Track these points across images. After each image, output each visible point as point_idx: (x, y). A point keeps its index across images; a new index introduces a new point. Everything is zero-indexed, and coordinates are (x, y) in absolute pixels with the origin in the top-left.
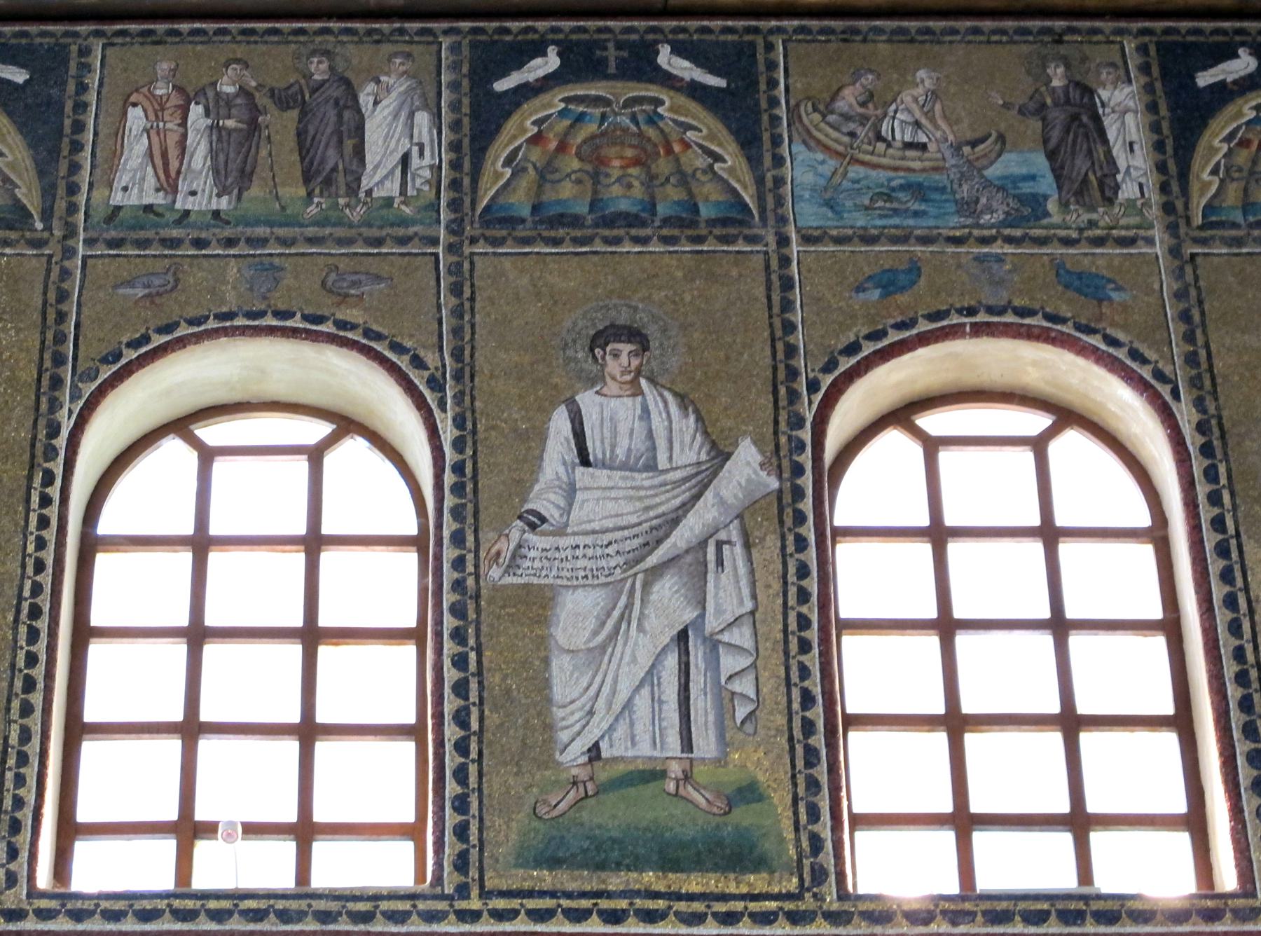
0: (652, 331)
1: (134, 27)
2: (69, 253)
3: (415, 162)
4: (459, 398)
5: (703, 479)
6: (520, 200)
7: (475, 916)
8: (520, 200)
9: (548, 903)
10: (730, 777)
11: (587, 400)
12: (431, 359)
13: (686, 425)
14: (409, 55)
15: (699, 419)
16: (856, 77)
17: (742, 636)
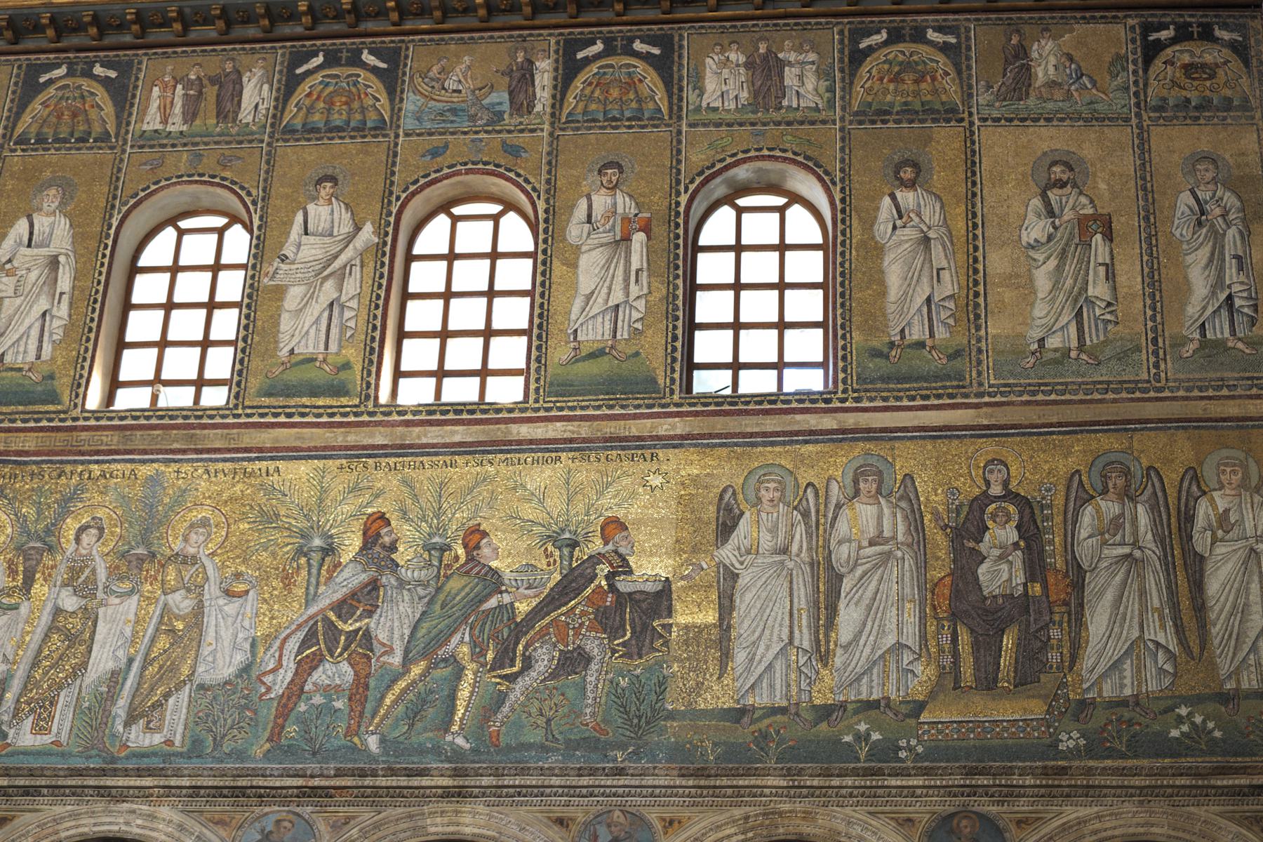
0: (340, 177)
1: (160, 51)
2: (124, 151)
3: (260, 107)
4: (262, 208)
5: (350, 238)
6: (298, 123)
7: (239, 416)
8: (298, 123)
9: (267, 410)
10: (340, 360)
11: (311, 208)
12: (254, 192)
13: (347, 216)
14: (264, 59)
15: (352, 214)
16: (439, 60)
17: (353, 304)
